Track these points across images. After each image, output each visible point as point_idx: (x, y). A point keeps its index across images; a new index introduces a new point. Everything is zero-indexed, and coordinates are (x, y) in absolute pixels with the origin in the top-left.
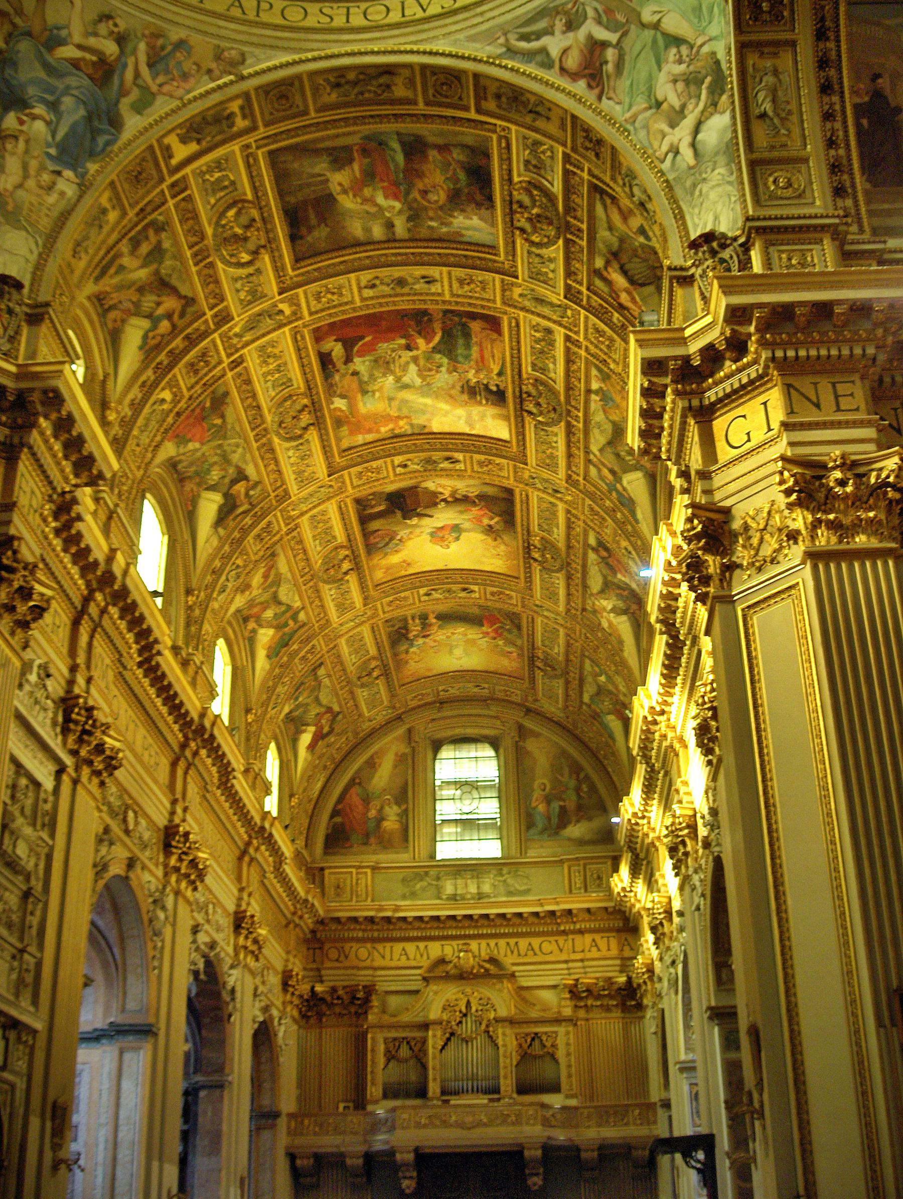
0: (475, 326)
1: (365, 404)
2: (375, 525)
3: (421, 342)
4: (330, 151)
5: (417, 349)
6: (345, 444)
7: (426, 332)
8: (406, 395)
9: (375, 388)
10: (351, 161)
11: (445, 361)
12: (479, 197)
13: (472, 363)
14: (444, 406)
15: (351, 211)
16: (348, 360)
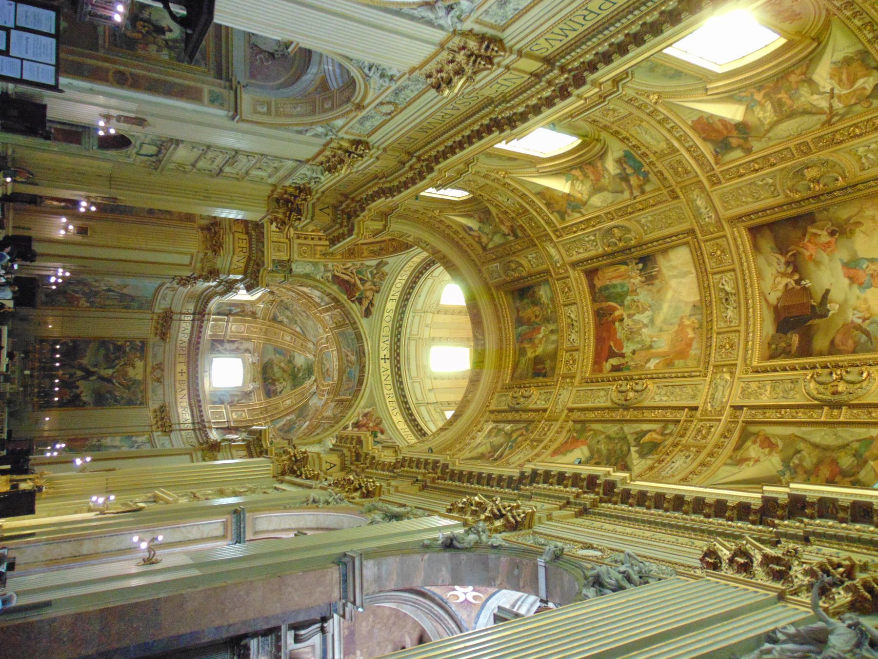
0: (598, 284)
1: (660, 347)
2: (820, 342)
3: (617, 313)
4: (519, 356)
5: (622, 315)
6: (695, 363)
7: (613, 309)
8: (659, 321)
9: (649, 340)
10: (524, 348)
11: (629, 298)
12: (531, 292)
13: (626, 281)
14: (669, 295)
15: (543, 350)
16: (623, 356)
